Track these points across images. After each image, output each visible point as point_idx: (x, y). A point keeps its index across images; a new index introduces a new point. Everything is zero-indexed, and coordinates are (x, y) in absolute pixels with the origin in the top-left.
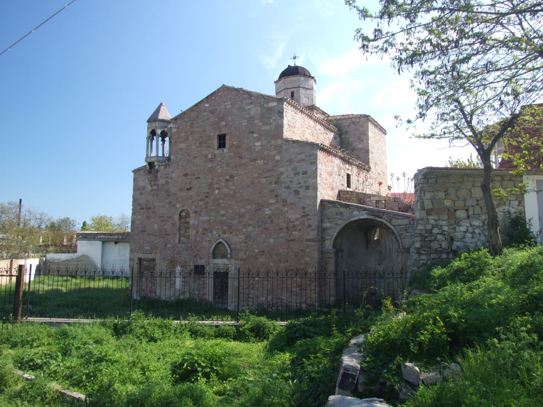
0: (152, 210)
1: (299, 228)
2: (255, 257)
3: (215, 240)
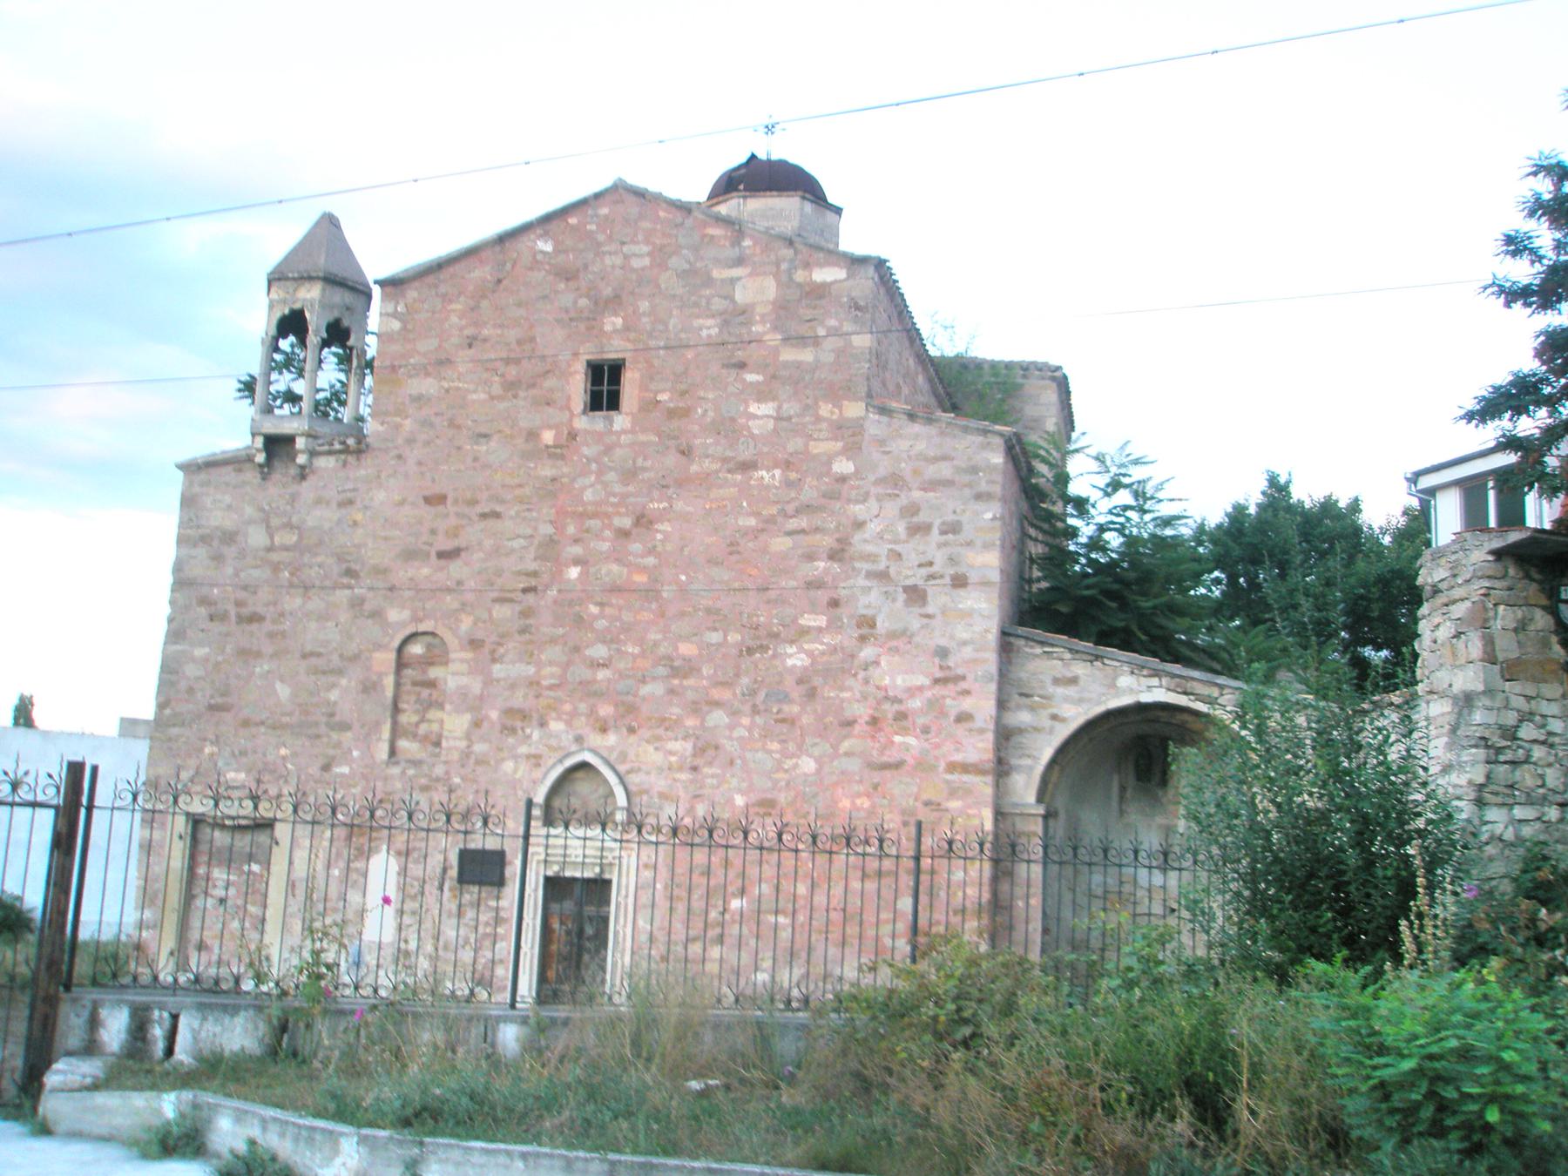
0: (268, 626)
1: (921, 721)
3: (558, 755)
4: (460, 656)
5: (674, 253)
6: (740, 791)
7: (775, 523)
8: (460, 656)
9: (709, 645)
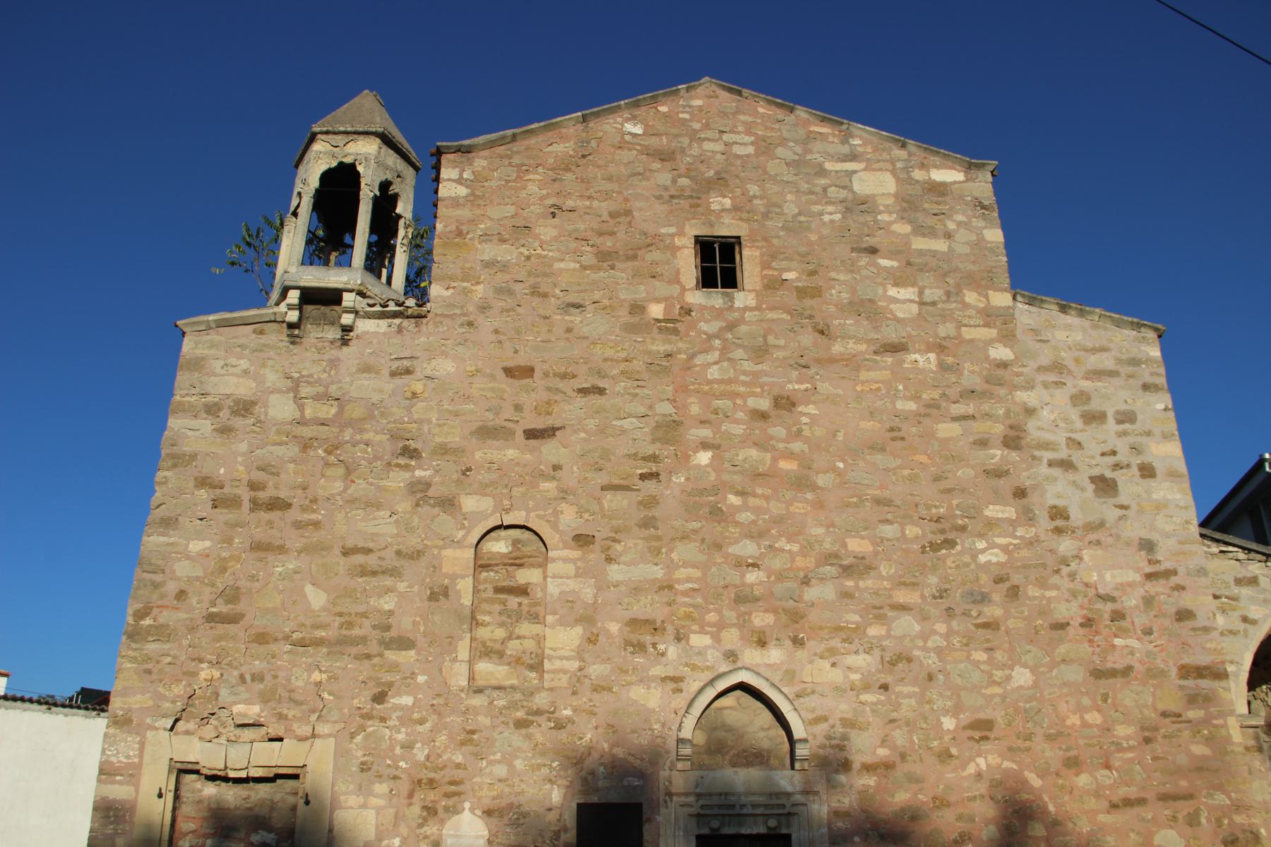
0: (294, 514)
1: (1140, 620)
2: (944, 756)
3: (708, 676)
5: (779, 145)
6: (946, 712)
7: (938, 408)
8: (563, 559)
9: (882, 539)
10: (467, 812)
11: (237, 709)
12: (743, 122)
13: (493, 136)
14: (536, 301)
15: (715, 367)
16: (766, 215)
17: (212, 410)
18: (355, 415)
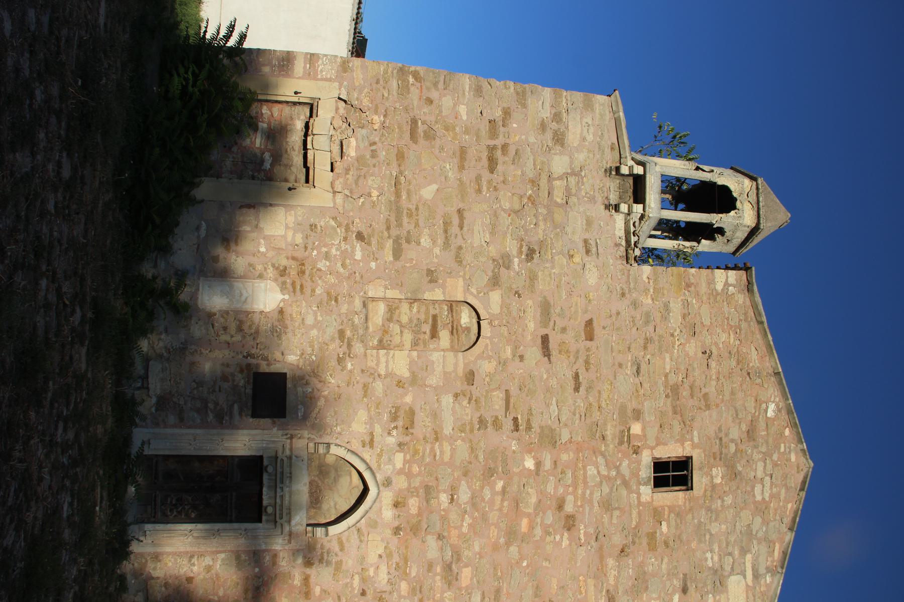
0: (486, 175)
3: (374, 465)
4: (457, 363)
5: (763, 519)
8: (457, 363)
10: (282, 297)
11: (353, 141)
12: (780, 492)
13: (761, 307)
14: (641, 342)
15: (595, 472)
16: (709, 509)
17: (557, 117)
18: (556, 216)
